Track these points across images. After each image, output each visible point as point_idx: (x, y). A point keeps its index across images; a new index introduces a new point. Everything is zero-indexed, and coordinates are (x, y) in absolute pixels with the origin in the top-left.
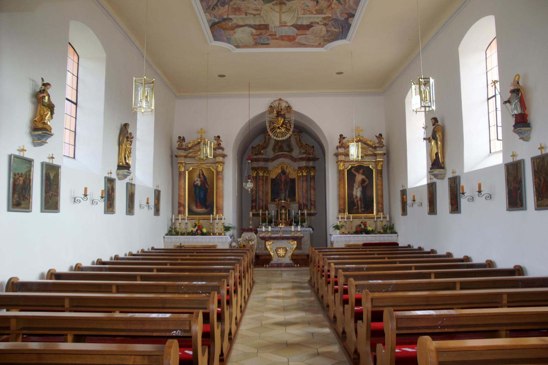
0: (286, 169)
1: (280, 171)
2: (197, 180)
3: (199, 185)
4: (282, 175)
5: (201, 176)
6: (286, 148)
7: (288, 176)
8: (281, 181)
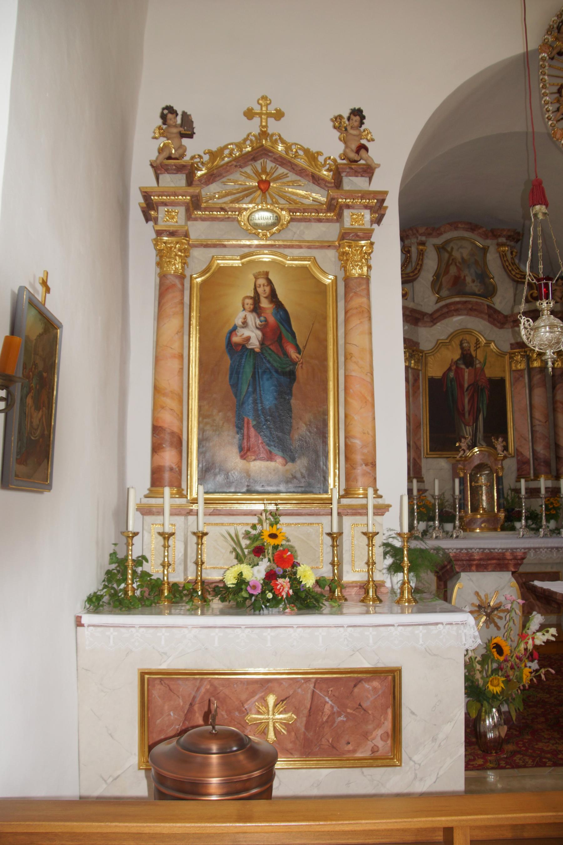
0: (476, 350)
1: (457, 356)
2: (245, 324)
3: (255, 343)
4: (463, 366)
5: (265, 303)
6: (472, 285)
7: (482, 370)
8: (461, 386)
